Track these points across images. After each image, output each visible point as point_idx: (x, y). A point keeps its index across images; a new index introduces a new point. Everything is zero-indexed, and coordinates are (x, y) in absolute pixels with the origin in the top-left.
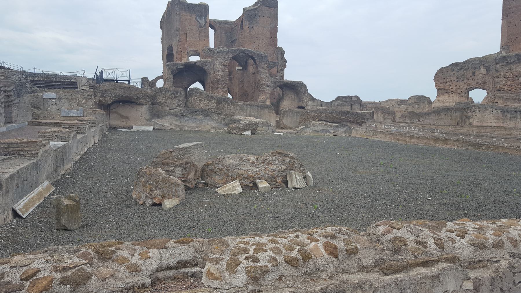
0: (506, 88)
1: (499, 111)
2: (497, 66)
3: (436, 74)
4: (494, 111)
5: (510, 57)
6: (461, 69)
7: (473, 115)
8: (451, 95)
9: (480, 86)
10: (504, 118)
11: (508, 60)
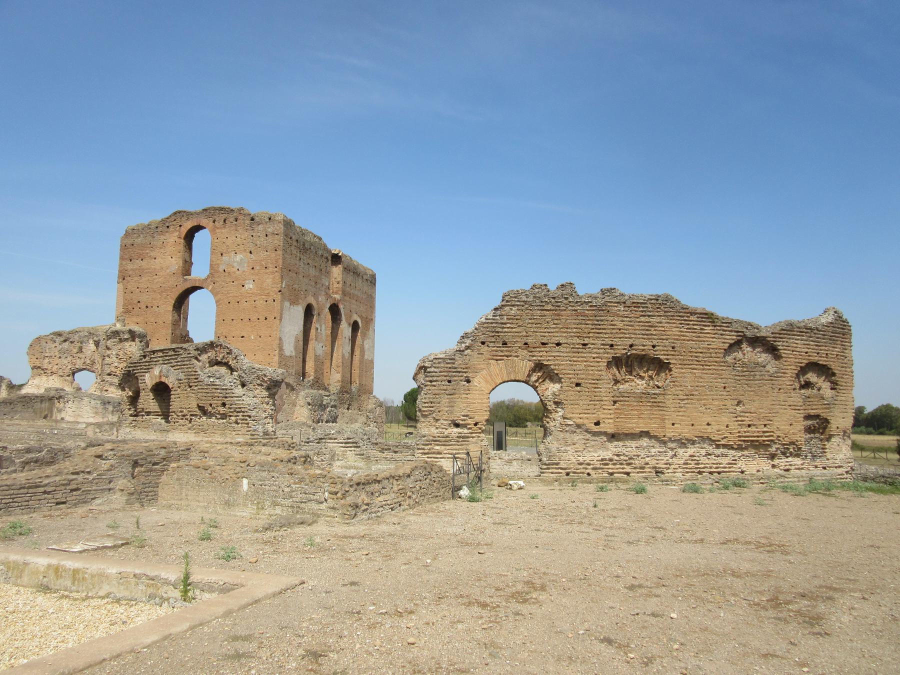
0: (118, 372)
1: (99, 402)
2: (108, 342)
4: (93, 402)
5: (123, 333)
6: (65, 341)
7: (65, 407)
8: (50, 378)
9: (88, 367)
10: (104, 411)
11: (122, 335)
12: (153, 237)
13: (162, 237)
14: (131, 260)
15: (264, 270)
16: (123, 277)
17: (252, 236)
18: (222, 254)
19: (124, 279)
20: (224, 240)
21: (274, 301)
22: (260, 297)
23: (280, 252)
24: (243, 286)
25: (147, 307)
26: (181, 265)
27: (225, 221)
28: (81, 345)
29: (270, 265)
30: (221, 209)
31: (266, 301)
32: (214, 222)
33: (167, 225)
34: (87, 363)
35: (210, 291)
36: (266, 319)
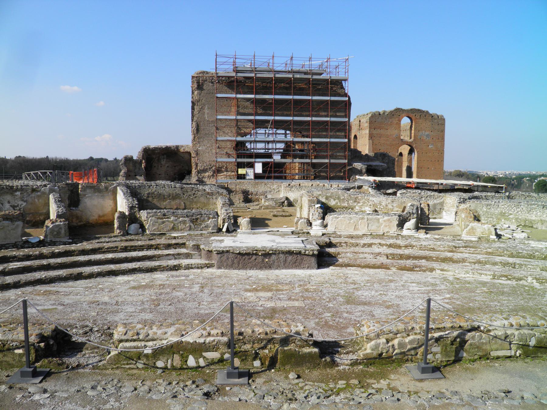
12: (386, 119)
15: (437, 140)
30: (419, 110)
33: (393, 114)
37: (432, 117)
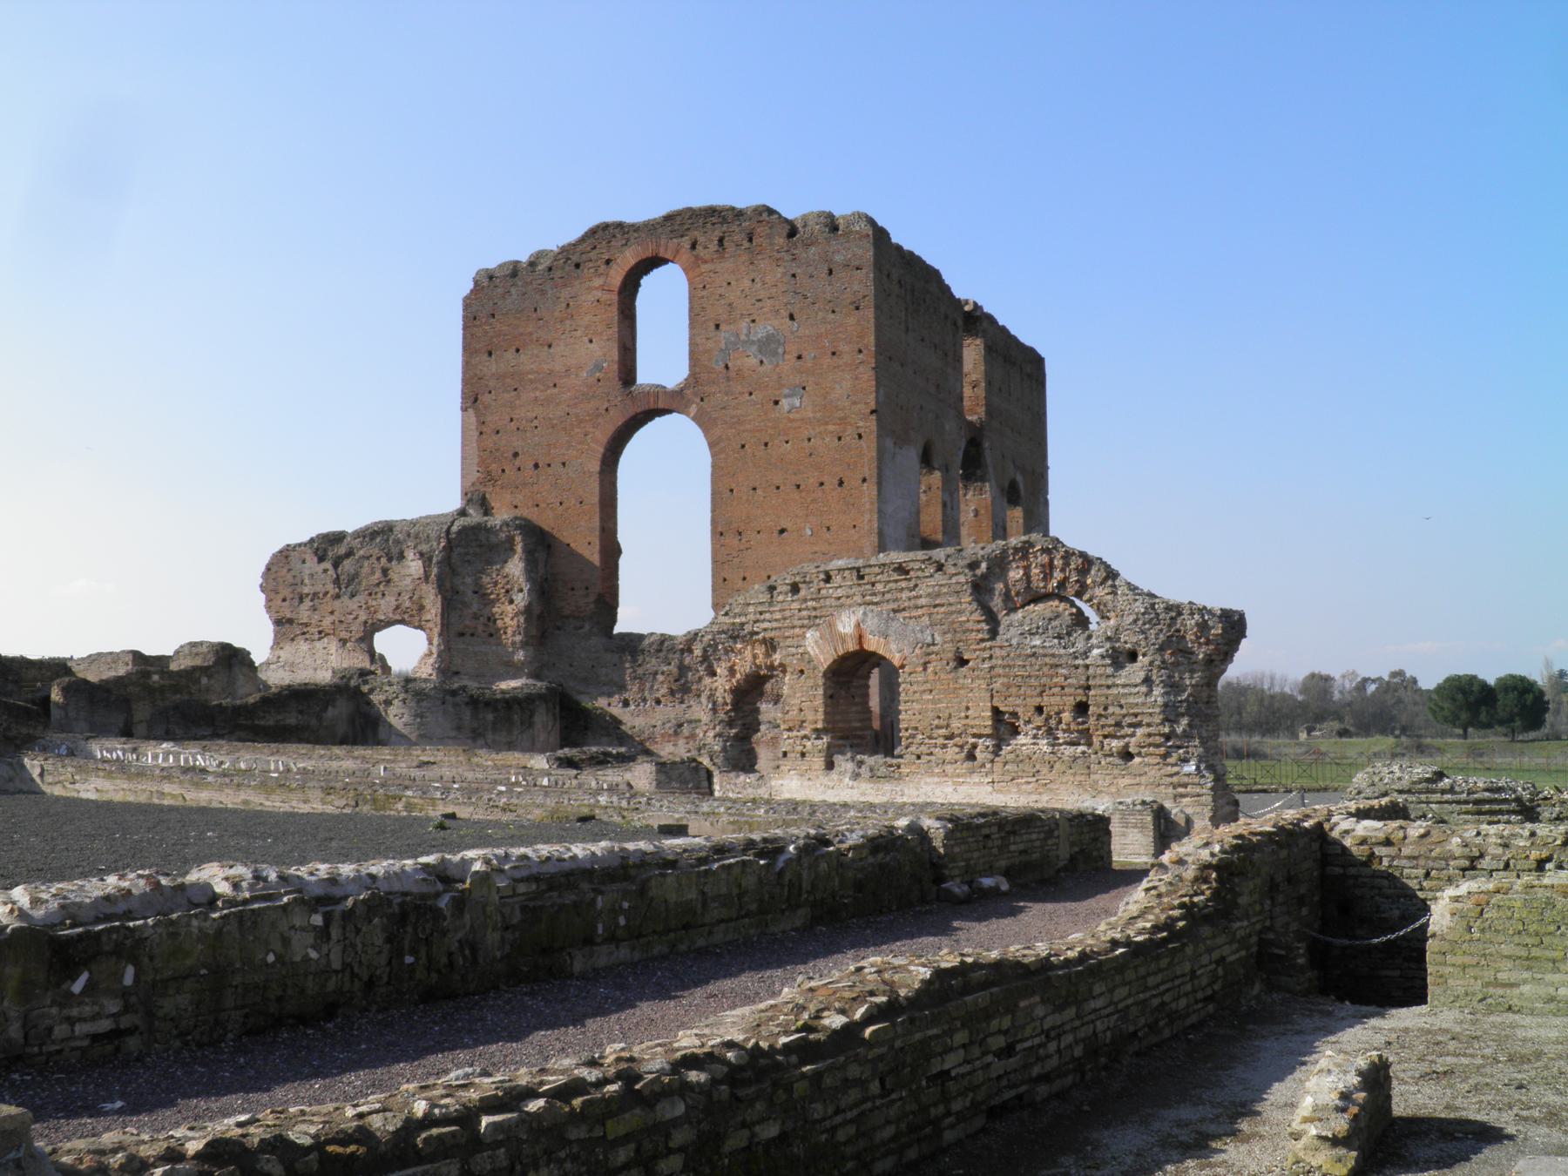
3: (268, 569)
8: (319, 645)
12: (543, 293)
13: (565, 293)
14: (490, 354)
15: (827, 360)
16: (472, 398)
17: (794, 275)
18: (717, 326)
19: (476, 400)
20: (721, 291)
21: (860, 436)
22: (822, 428)
23: (870, 314)
24: (776, 403)
25: (536, 466)
26: (616, 358)
27: (721, 240)
28: (388, 565)
29: (843, 347)
30: (712, 211)
31: (840, 439)
32: (694, 246)
33: (575, 258)
34: (403, 607)
35: (694, 419)
36: (841, 483)
37: (793, 232)
